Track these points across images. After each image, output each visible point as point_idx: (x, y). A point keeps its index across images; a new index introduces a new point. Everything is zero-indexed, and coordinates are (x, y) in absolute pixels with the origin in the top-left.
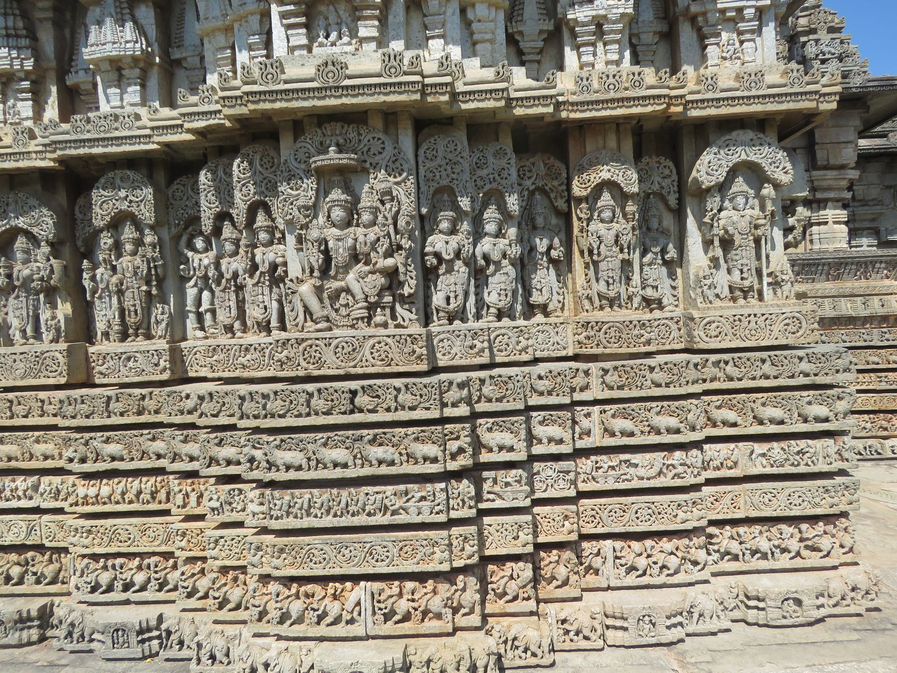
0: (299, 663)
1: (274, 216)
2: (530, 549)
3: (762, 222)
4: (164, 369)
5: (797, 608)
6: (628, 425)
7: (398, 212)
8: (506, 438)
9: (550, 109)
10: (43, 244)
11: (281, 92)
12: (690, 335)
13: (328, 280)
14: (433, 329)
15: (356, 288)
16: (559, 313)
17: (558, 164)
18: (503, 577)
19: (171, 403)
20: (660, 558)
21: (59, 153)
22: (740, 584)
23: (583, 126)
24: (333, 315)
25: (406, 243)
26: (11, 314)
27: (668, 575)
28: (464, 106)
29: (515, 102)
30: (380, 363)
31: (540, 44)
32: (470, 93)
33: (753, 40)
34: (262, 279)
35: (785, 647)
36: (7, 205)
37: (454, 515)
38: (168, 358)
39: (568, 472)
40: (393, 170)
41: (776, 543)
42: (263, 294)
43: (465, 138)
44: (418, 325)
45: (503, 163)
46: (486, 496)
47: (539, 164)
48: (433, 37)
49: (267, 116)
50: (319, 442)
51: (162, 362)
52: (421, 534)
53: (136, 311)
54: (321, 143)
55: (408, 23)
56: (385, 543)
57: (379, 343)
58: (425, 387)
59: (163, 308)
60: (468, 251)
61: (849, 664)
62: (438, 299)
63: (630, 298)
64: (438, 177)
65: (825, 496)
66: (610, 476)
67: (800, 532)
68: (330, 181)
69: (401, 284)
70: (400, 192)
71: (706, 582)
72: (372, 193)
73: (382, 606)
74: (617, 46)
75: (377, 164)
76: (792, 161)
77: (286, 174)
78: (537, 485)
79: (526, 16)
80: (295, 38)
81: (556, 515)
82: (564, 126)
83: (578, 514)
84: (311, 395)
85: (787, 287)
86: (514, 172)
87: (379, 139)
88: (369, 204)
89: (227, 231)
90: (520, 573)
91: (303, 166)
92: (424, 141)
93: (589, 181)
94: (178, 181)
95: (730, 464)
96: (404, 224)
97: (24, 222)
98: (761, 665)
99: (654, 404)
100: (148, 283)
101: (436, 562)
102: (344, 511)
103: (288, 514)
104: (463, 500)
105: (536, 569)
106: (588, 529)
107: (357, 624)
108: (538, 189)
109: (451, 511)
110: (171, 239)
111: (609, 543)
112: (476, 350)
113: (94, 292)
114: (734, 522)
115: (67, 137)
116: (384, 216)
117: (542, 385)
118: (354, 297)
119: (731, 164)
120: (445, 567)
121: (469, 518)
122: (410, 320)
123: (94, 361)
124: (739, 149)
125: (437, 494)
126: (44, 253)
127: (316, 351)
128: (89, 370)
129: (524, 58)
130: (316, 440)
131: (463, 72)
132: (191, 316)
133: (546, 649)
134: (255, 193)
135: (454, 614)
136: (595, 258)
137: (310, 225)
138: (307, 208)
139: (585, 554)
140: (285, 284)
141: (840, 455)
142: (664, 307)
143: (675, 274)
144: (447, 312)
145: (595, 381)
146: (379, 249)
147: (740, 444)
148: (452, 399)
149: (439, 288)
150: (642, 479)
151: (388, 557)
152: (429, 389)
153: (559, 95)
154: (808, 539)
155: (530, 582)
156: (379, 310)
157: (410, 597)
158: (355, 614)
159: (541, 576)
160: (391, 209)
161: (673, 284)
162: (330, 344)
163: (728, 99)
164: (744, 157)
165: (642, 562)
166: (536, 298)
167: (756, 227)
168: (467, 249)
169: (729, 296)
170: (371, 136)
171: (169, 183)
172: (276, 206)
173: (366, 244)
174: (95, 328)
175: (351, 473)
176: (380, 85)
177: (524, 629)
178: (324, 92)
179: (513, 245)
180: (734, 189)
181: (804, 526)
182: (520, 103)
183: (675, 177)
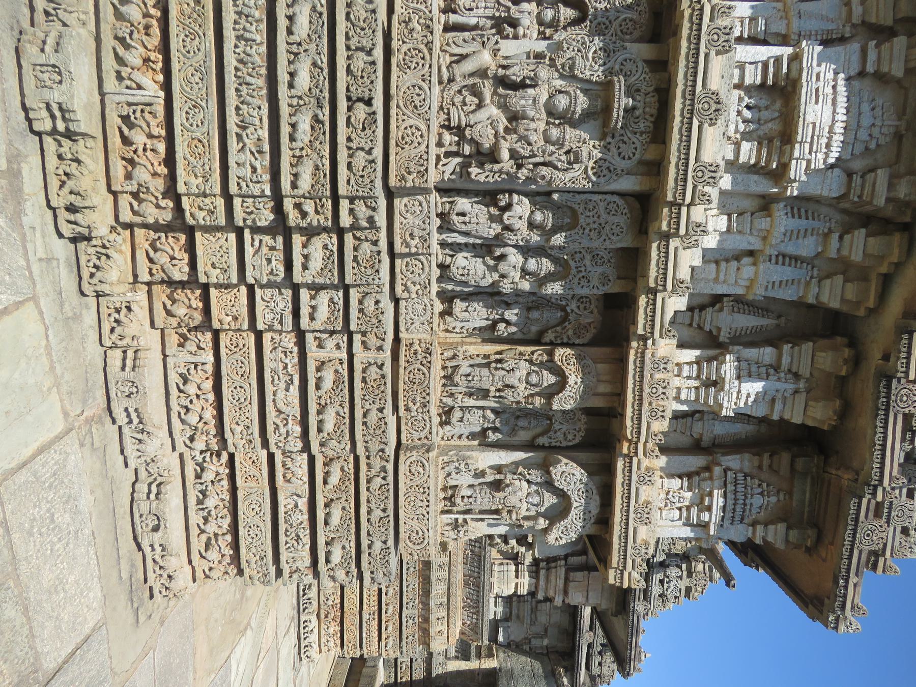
0: (69, 9)
1: (569, 29)
2: (203, 279)
3: (514, 517)
5: (150, 527)
6: (328, 384)
7: (556, 168)
8: (316, 263)
9: (640, 331)
11: (698, 49)
12: (414, 448)
13: (493, 85)
14: (433, 196)
15: (482, 115)
16: (442, 327)
17: (588, 336)
18: (173, 249)
20: (197, 406)
22: (172, 479)
23: (623, 361)
24: (456, 87)
25: (523, 174)
27: (179, 413)
28: (654, 246)
29: (652, 297)
30: (400, 134)
31: (707, 328)
32: (667, 253)
33: (680, 519)
34: (502, 8)
35: (111, 514)
37: (237, 202)
39: (281, 323)
40: (600, 167)
41: (213, 513)
42: (485, 8)
43: (624, 245)
44: (438, 180)
45: (595, 282)
46: (257, 238)
47: (591, 318)
48: (729, 220)
49: (676, 32)
50: (317, 58)
52: (217, 164)
54: (638, 90)
55: (749, 195)
56: (206, 123)
57: (422, 136)
58: (372, 182)
60: (509, 239)
61: (96, 568)
62: (463, 203)
63: (452, 395)
64: (588, 214)
65: (258, 557)
66: (278, 364)
67: (223, 534)
68: (598, 96)
69: (481, 165)
70: (577, 172)
71: (174, 449)
72: (579, 142)
73: (138, 114)
74: (693, 399)
75: (609, 150)
76: (564, 546)
77: (611, 47)
78: (269, 292)
79: (736, 315)
80: (753, 71)
81: (238, 308)
82: (625, 344)
83: (239, 330)
84: (369, 53)
85: (452, 535)
86: (584, 292)
87: (634, 154)
88: (567, 137)
90: (177, 268)
91: (617, 67)
92: (627, 203)
93: (568, 364)
95: (288, 476)
96: (543, 173)
98: (92, 492)
99: (347, 410)
101: (187, 179)
102: (241, 80)
103: (239, 13)
104: (251, 213)
105: (182, 284)
106: (224, 340)
107: (117, 83)
108: (567, 314)
109: (240, 200)
111: (211, 359)
112: (408, 239)
114: (232, 477)
116: (553, 153)
117: (369, 304)
118: (472, 112)
119: (569, 493)
120: (181, 188)
121: (233, 218)
122: (443, 172)
124: (583, 501)
125: (259, 185)
129: (696, 311)
130: (320, 54)
131: (688, 248)
133: (98, 288)
134: (596, 9)
135: (132, 193)
136: (493, 365)
137: (553, 69)
138: (572, 68)
139: (199, 335)
140: (494, 35)
141: (296, 571)
142: (441, 426)
143: (473, 439)
144: (449, 212)
145: (371, 356)
146: (519, 144)
147: (307, 486)
148: (357, 209)
149: (475, 205)
150: (274, 395)
151: (191, 125)
152: (369, 186)
153: (654, 340)
154: (217, 540)
155: (169, 277)
156: (457, 139)
157: (148, 146)
158: (128, 83)
159: (176, 289)
160: (560, 160)
161: (464, 437)
162: (423, 80)
163: (629, 493)
164: (575, 504)
165: (192, 389)
166: (459, 306)
167: (510, 512)
168: (512, 238)
169: (448, 485)
170: (638, 145)
172: (579, 33)
173: (527, 130)
175: (283, 91)
176: (687, 159)
177: (118, 266)
178: (690, 97)
179: (512, 286)
180: (547, 495)
181: (229, 538)
182: (651, 302)
183: (564, 444)
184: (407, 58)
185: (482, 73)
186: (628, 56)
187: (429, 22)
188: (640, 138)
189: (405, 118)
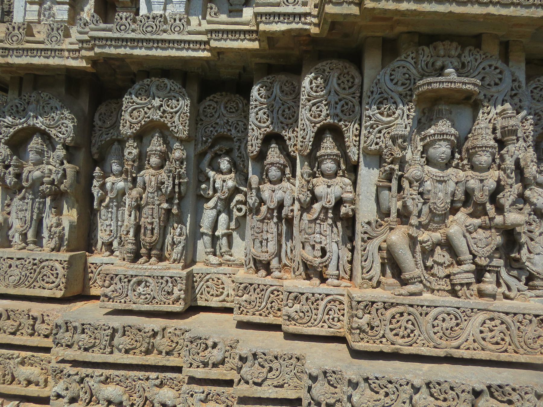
4: (178, 300)
10: (59, 146)
15: (461, 244)
19: (193, 351)
21: (97, 50)
26: (13, 214)
36: (28, 103)
38: (184, 287)
51: (176, 290)
53: (153, 229)
57: (492, 319)
59: (181, 228)
77: (376, 96)
87: (496, 68)
89: (274, 154)
91: (401, 89)
94: (211, 97)
97: (42, 123)
100: (170, 200)
110: (195, 156)
113: (102, 201)
115: (109, 34)
123: (92, 272)
126: (58, 156)
127: (407, 322)
128: (86, 281)
132: (207, 239)
134: (328, 115)
146: (502, 201)
156: (487, 275)
162: (427, 314)
171: (201, 99)
172: (350, 131)
174: (96, 236)
184: (401, 334)
185: (413, 241)
186: (387, 78)
187: (362, 305)
188: (479, 61)
189: (471, 339)
